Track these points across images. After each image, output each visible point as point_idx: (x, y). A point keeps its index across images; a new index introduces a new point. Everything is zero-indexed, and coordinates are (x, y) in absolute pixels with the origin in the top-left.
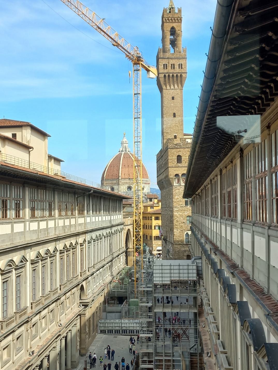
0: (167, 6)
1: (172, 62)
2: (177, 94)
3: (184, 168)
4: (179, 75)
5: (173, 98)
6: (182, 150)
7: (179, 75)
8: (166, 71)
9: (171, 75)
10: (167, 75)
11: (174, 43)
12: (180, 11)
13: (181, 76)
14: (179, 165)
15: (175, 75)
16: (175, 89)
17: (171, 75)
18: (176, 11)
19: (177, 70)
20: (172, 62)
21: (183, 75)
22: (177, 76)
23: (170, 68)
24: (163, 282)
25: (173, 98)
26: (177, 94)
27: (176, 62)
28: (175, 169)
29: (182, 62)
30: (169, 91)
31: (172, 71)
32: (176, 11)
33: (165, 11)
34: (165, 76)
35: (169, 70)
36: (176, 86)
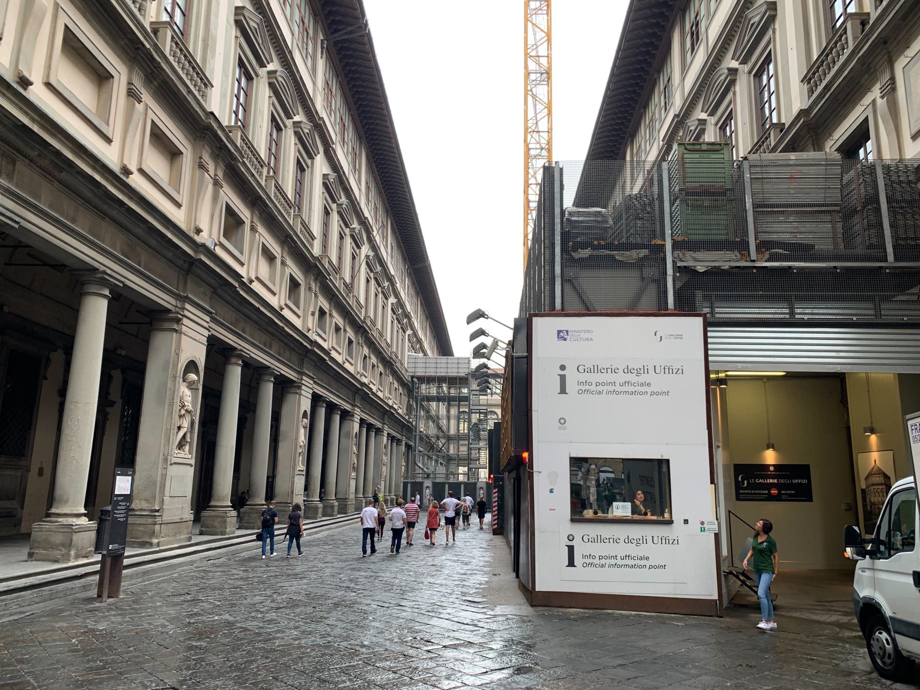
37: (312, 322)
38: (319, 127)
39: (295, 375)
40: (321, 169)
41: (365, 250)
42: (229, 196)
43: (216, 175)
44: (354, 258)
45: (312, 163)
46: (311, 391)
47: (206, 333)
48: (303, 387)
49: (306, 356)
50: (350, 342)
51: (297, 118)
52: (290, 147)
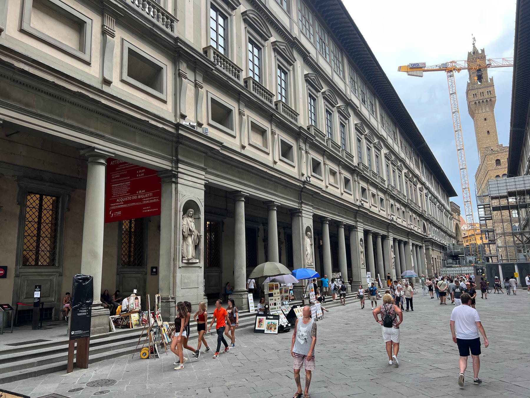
0: (471, 50)
1: (480, 91)
2: (489, 115)
3: (503, 170)
4: (488, 100)
5: (485, 119)
6: (500, 154)
7: (488, 100)
8: (476, 99)
9: (481, 101)
10: (477, 102)
11: (480, 78)
12: (483, 51)
13: (490, 100)
14: (499, 167)
15: (485, 101)
16: (486, 112)
17: (481, 101)
18: (480, 52)
19: (486, 96)
20: (480, 91)
21: (493, 99)
22: (487, 101)
23: (480, 96)
24: (500, 194)
25: (485, 119)
26: (489, 115)
27: (485, 91)
28: (495, 171)
29: (489, 89)
30: (482, 113)
31: (482, 97)
32: (480, 52)
33: (469, 54)
34: (475, 103)
35: (479, 97)
36: (487, 109)
37: (307, 170)
38: (294, 44)
39: (297, 205)
40: (302, 71)
41: (353, 120)
42: (210, 92)
43: (195, 80)
44: (342, 125)
45: (294, 69)
46: (312, 214)
47: (203, 182)
48: (303, 212)
49: (302, 191)
50: (347, 181)
51: (272, 39)
52: (270, 59)
